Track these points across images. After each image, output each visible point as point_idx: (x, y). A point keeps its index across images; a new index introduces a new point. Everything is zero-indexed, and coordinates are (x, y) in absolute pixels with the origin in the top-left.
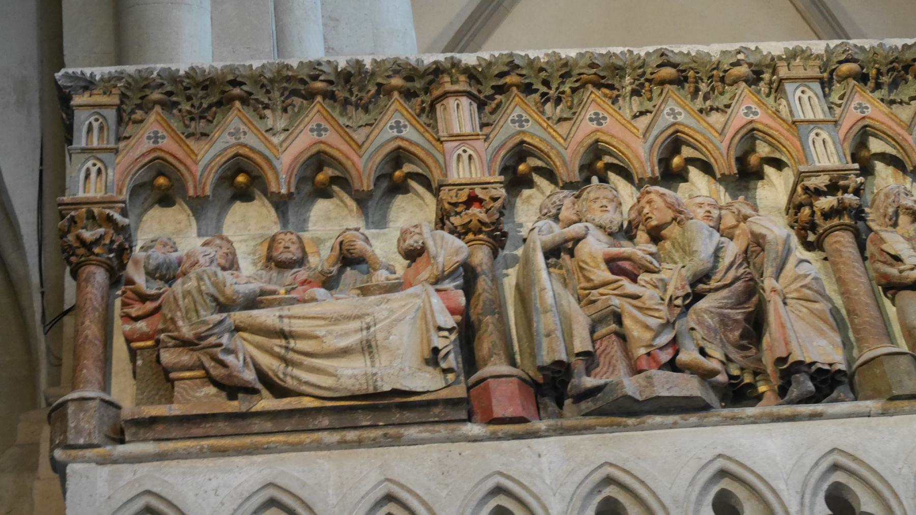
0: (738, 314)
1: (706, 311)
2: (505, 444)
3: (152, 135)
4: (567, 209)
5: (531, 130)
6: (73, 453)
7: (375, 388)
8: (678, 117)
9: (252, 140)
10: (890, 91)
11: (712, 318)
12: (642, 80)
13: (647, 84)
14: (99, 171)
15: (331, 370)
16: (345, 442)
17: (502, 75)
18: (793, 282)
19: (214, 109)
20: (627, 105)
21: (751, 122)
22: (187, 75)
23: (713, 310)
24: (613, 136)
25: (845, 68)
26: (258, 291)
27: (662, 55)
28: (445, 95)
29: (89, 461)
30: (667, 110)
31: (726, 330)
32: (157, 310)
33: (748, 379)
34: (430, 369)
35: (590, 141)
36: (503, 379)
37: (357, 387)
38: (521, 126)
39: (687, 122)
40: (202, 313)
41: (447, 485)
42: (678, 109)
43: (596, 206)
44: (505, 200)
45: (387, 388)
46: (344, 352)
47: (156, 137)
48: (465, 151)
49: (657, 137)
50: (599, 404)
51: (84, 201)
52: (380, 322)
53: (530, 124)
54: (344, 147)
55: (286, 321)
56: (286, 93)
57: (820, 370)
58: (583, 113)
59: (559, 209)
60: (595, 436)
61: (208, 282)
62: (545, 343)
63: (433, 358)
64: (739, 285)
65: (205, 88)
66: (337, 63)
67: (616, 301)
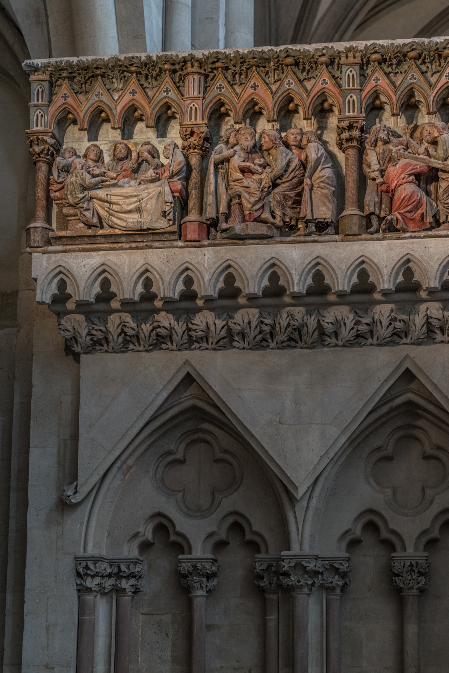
0: (292, 194)
1: (278, 193)
2: (192, 249)
3: (64, 95)
4: (232, 138)
5: (224, 93)
6: (33, 249)
7: (141, 227)
8: (291, 85)
9: (104, 98)
10: (396, 68)
11: (280, 197)
12: (278, 64)
13: (280, 66)
14: (42, 115)
15: (125, 219)
16: (132, 248)
17: (213, 63)
18: (317, 179)
19: (91, 79)
20: (272, 76)
21: (324, 88)
22: (77, 65)
23: (281, 193)
24: (260, 97)
25: (374, 57)
26: (100, 180)
27: (287, 51)
28: (188, 74)
29: (39, 252)
30: (286, 82)
31: (286, 201)
32: (63, 188)
33: (293, 222)
34: (164, 218)
35: (249, 99)
36: (193, 223)
37: (134, 227)
38: (220, 91)
39: (294, 88)
40: (77, 193)
41: (169, 266)
42: (292, 81)
43: (243, 137)
44: (206, 133)
45: (145, 227)
46: (130, 212)
47: (65, 97)
48: (194, 105)
49: (279, 98)
50: (228, 235)
51: (36, 132)
52: (144, 198)
53: (224, 89)
54: (143, 102)
55: (109, 196)
56: (121, 72)
57: (318, 222)
58: (248, 84)
59: (229, 138)
60: (227, 247)
61: (79, 178)
62: (208, 207)
63: (164, 214)
64: (295, 180)
65: (85, 70)
66: (141, 57)
67: (240, 189)
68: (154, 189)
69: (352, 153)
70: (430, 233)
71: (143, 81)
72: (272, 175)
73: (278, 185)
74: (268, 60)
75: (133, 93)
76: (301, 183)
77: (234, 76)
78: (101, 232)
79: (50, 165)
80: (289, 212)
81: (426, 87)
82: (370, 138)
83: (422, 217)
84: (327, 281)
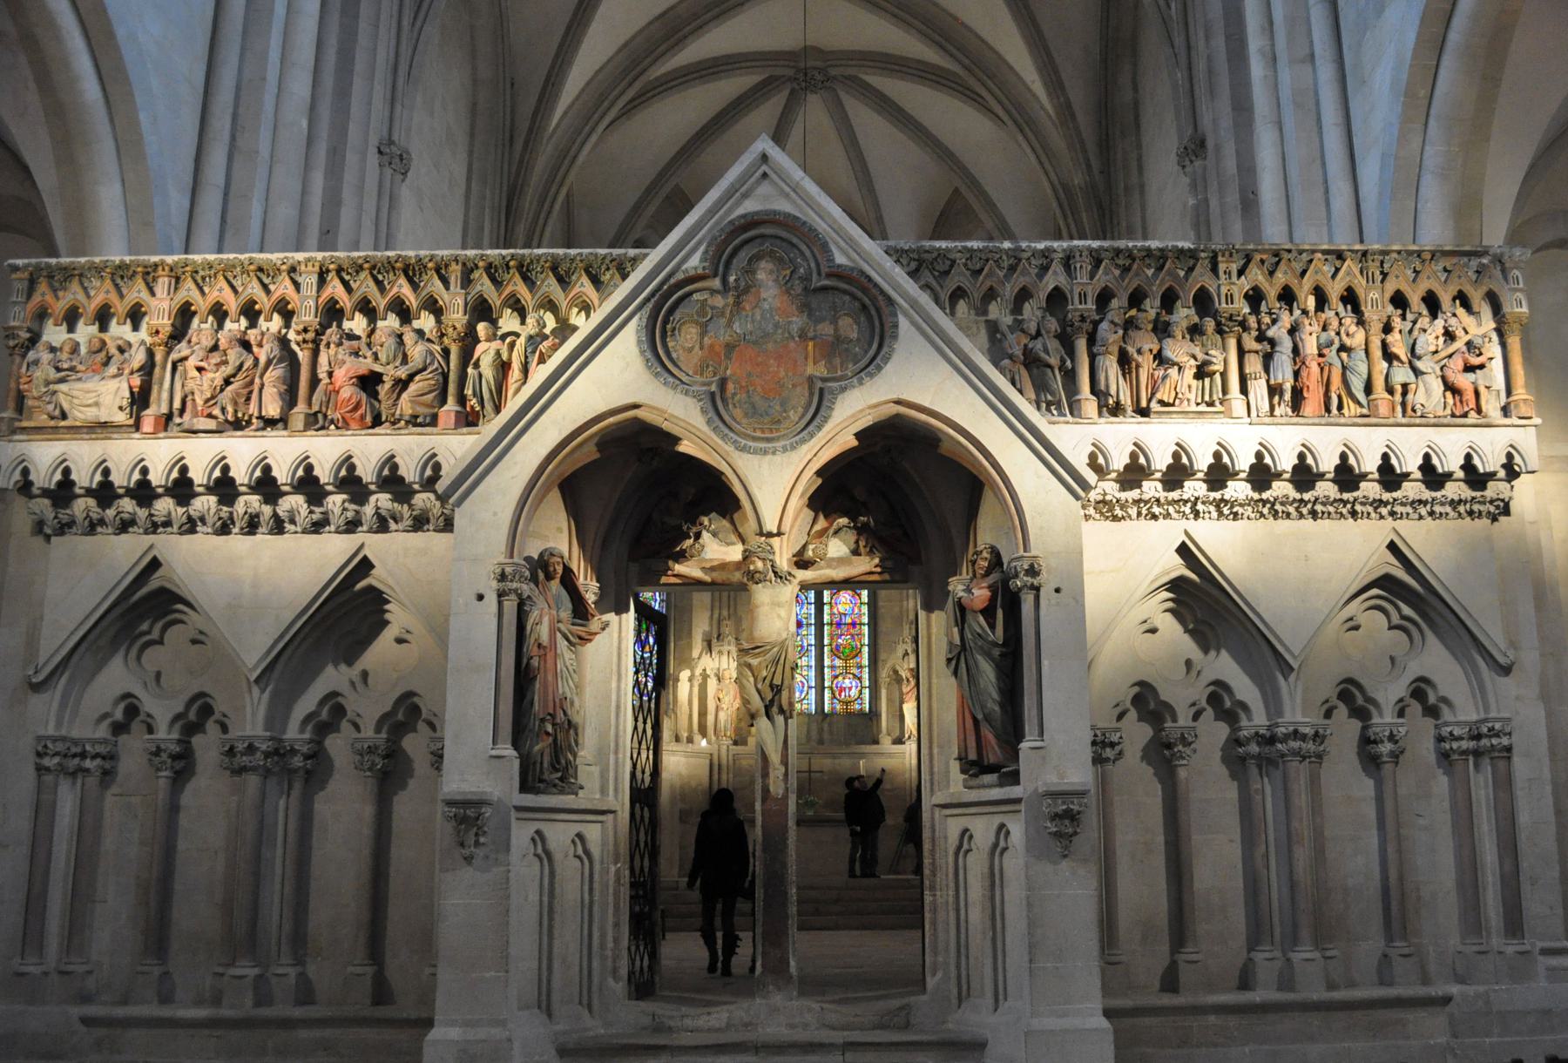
0: (245, 391)
68: (113, 384)
70: (370, 431)
71: (119, 281)
72: (225, 375)
73: (231, 383)
74: (234, 266)
75: (107, 292)
76: (252, 383)
77: (203, 278)
78: (63, 423)
79: (24, 356)
81: (378, 294)
83: (363, 417)
84: (274, 473)
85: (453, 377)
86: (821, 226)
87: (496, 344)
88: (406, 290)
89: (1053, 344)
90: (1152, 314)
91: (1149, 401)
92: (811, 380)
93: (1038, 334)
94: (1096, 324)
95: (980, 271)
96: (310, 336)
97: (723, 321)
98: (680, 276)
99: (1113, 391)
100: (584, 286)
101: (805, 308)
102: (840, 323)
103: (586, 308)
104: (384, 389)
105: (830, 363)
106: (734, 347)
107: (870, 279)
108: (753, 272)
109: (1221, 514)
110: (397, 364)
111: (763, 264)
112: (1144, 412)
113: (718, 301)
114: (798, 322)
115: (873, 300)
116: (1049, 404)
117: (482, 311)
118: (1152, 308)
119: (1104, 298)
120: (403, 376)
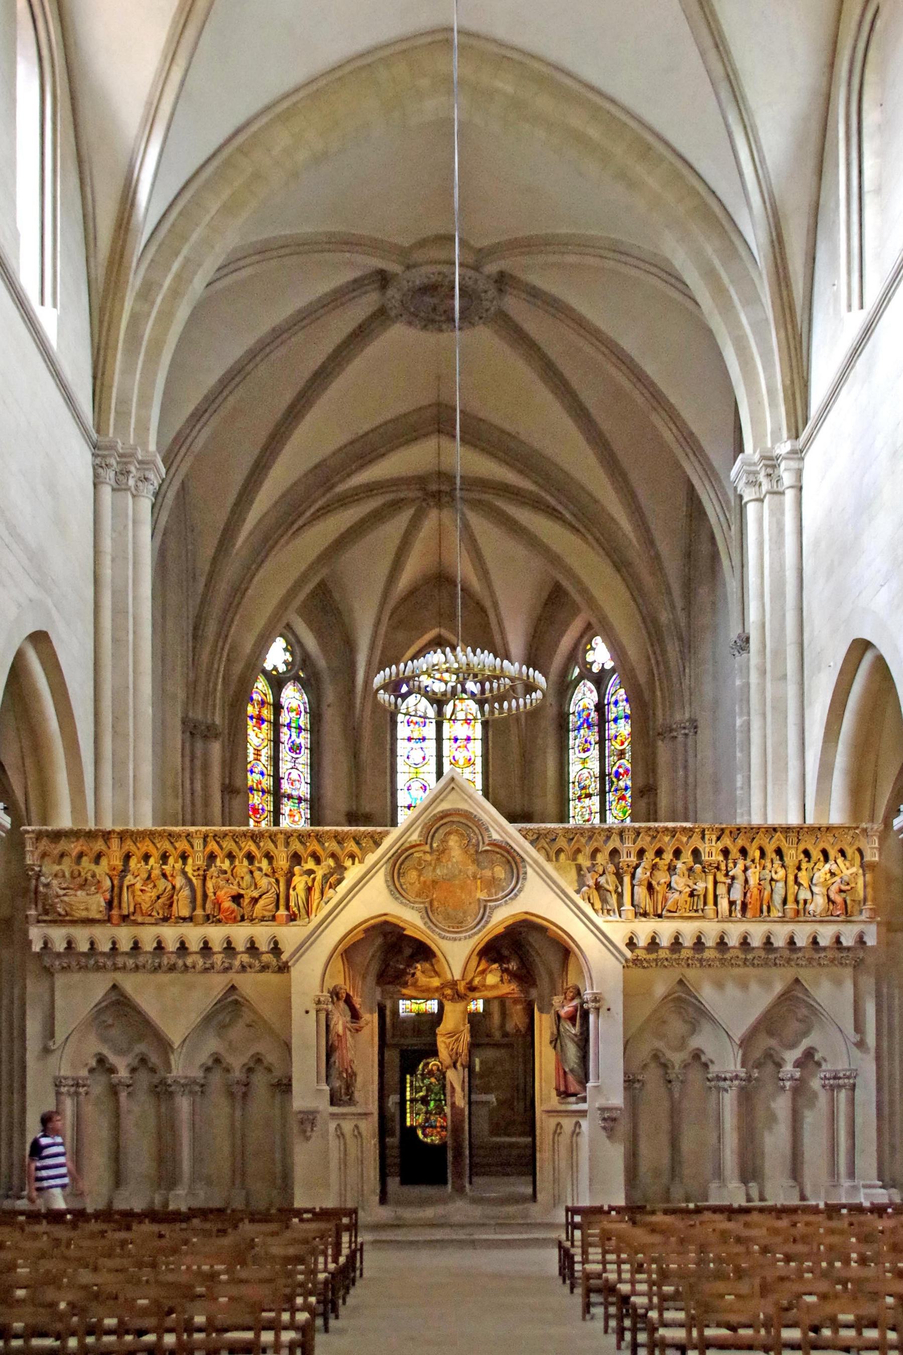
0: (168, 902)
69: (200, 882)
76: (172, 897)
80: (166, 911)
82: (209, 873)
83: (235, 918)
85: (282, 896)
86: (485, 817)
87: (305, 877)
88: (253, 848)
89: (612, 879)
90: (667, 861)
91: (662, 910)
92: (479, 900)
93: (604, 873)
94: (636, 868)
95: (572, 839)
96: (201, 872)
97: (431, 868)
98: (407, 845)
99: (642, 905)
100: (351, 846)
101: (476, 862)
102: (495, 869)
103: (352, 856)
104: (246, 901)
105: (489, 891)
106: (437, 883)
107: (512, 848)
108: (447, 842)
109: (701, 965)
110: (253, 888)
111: (452, 837)
112: (660, 916)
113: (428, 857)
114: (471, 869)
115: (513, 858)
116: (608, 911)
117: (296, 859)
118: (668, 856)
119: (641, 853)
120: (257, 896)
